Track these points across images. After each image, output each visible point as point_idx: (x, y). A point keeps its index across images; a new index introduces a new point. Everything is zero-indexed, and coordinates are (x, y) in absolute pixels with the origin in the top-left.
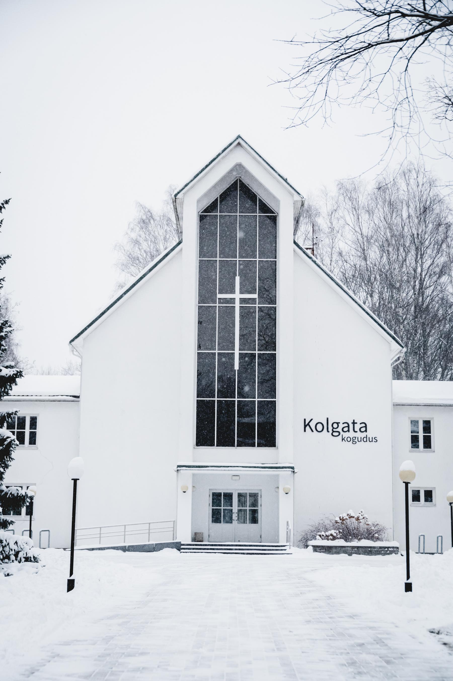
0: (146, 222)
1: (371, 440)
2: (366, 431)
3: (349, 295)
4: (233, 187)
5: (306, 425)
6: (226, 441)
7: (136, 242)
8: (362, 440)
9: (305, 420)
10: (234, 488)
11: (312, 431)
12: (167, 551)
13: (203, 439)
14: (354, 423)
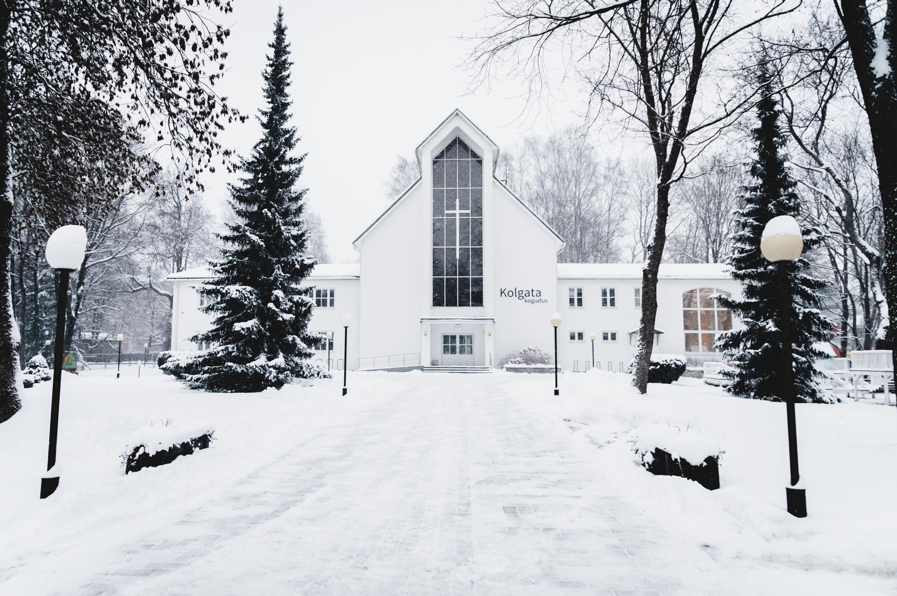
0: (402, 167)
4: (454, 142)
6: (451, 303)
7: (397, 180)
10: (458, 333)
12: (415, 371)
13: (437, 302)
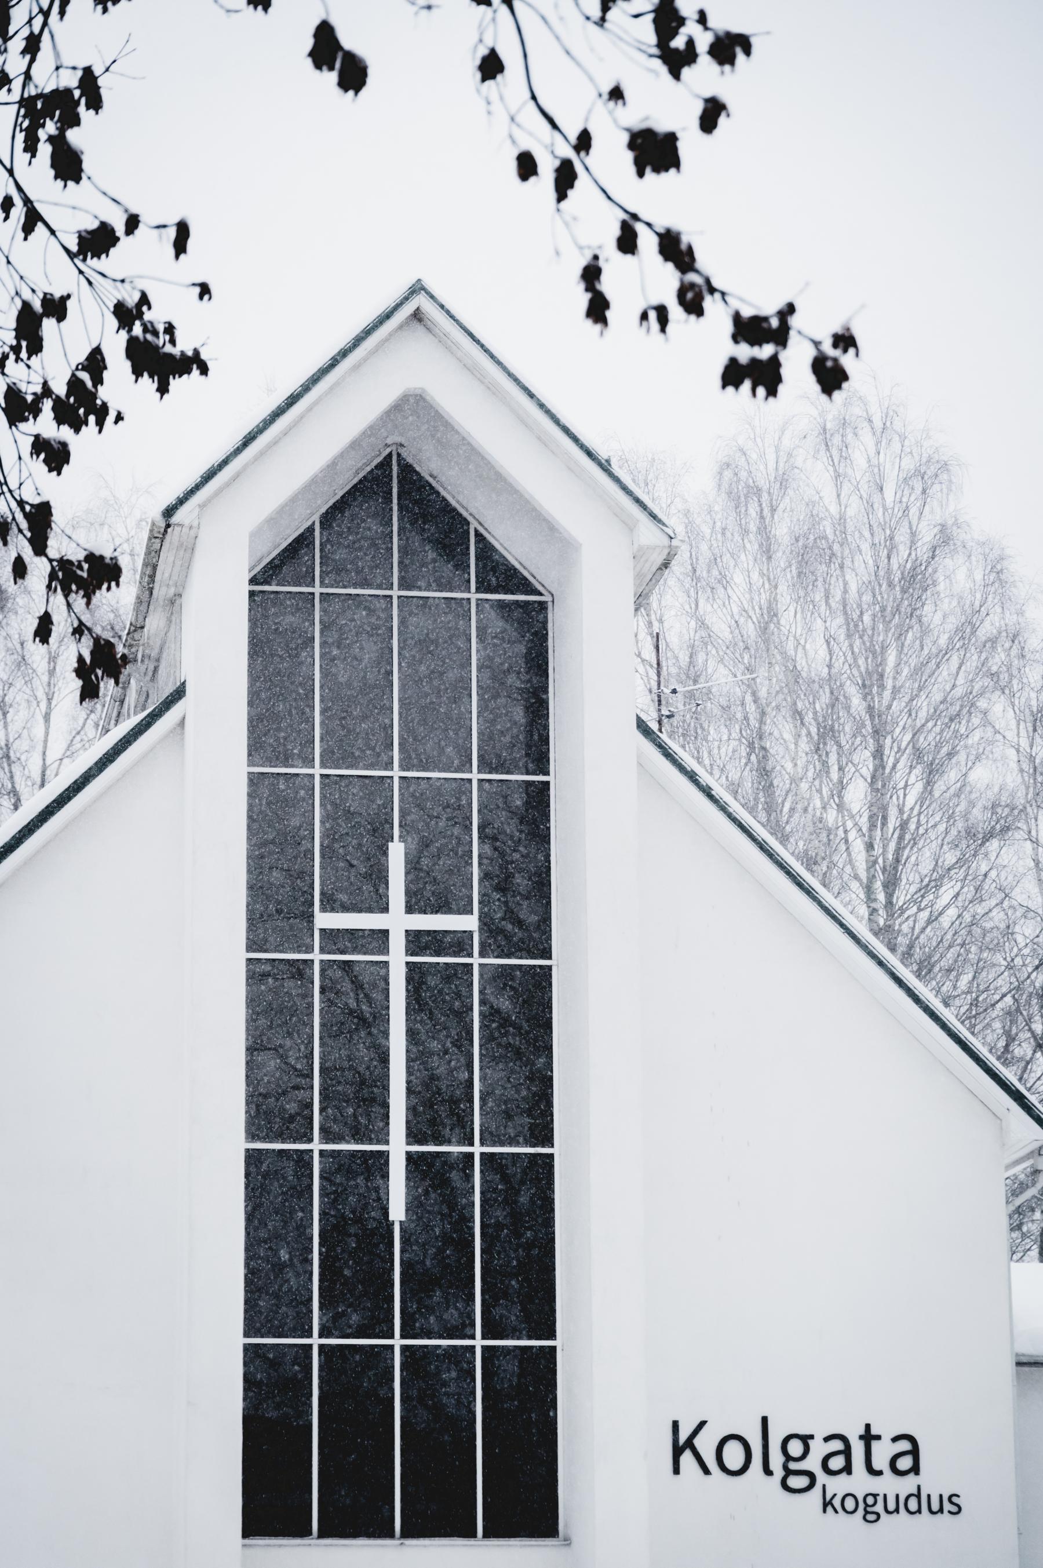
1: (935, 1507)
2: (915, 1469)
3: (842, 925)
5: (682, 1447)
8: (900, 1506)
9: (675, 1425)
11: (706, 1471)
14: (868, 1437)
